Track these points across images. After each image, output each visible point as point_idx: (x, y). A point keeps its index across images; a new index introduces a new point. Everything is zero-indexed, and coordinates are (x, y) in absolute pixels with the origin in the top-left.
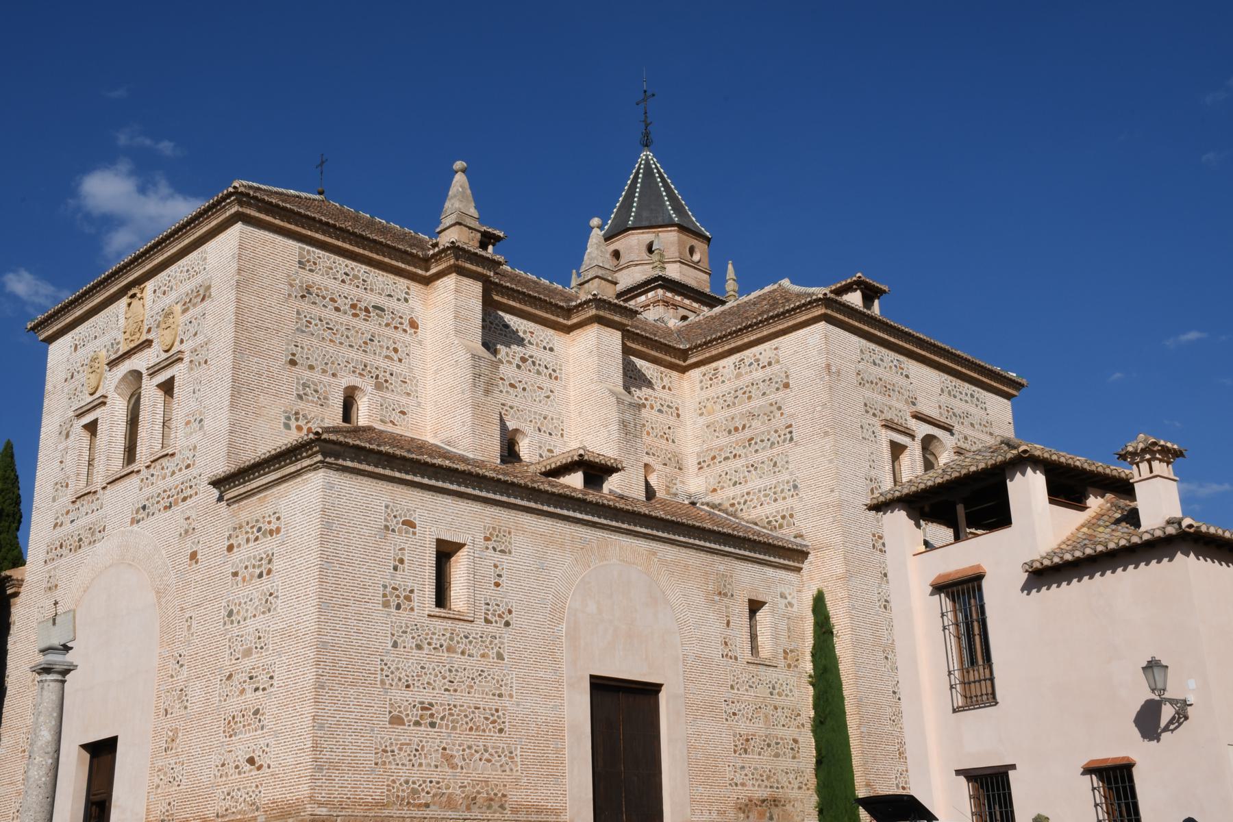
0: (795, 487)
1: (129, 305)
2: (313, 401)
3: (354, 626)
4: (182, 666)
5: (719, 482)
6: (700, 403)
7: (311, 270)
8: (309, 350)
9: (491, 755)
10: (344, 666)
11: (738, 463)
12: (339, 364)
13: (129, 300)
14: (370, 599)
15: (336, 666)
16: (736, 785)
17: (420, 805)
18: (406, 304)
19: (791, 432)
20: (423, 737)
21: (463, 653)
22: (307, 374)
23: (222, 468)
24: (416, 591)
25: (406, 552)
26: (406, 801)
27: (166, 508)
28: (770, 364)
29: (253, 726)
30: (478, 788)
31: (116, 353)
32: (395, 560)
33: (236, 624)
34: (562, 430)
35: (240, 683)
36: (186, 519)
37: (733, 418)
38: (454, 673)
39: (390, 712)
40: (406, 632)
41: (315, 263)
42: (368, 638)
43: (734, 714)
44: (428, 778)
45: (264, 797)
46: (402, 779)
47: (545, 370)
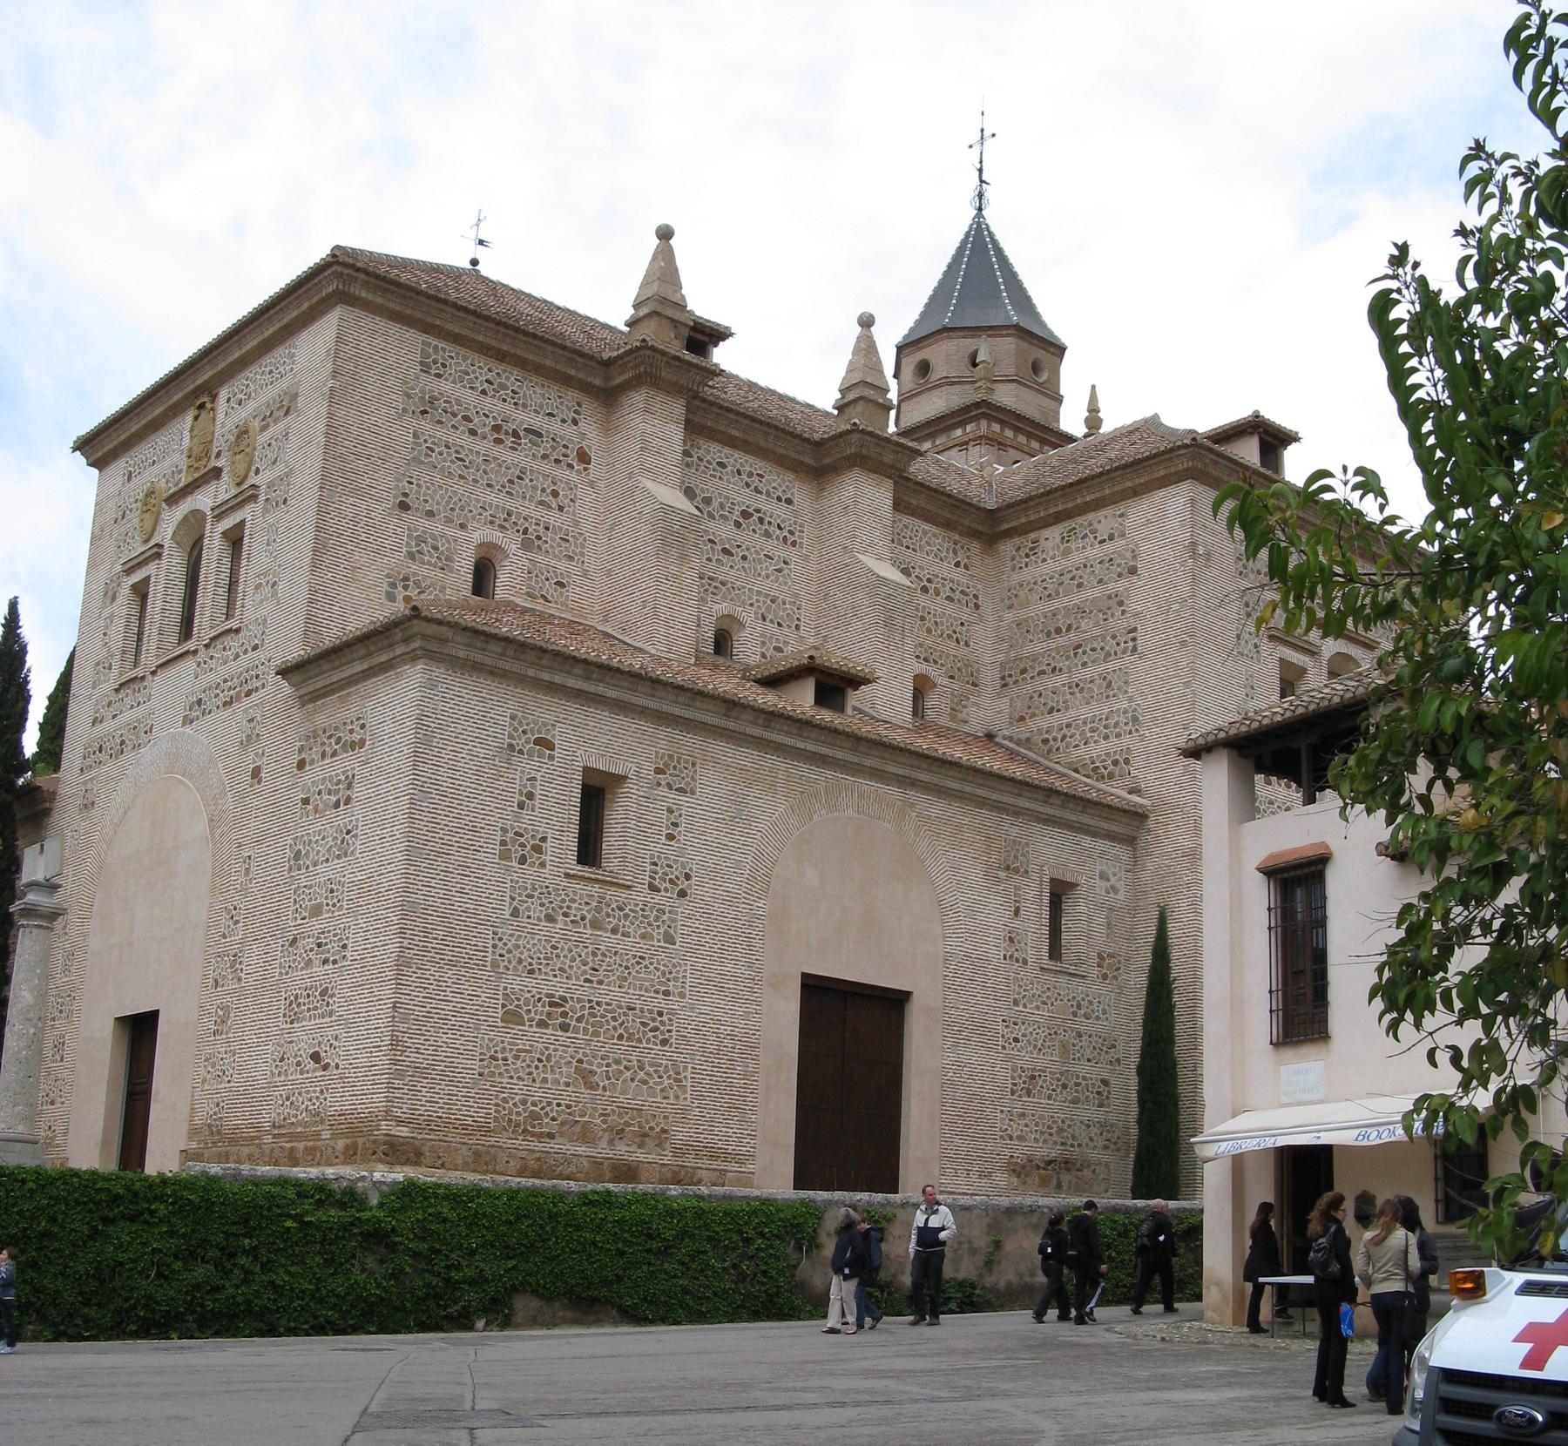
0: (1135, 719)
1: (196, 418)
2: (430, 563)
3: (457, 883)
4: (237, 922)
5: (1030, 707)
6: (1009, 590)
7: (438, 376)
8: (428, 488)
9: (648, 1074)
10: (440, 937)
11: (1059, 680)
12: (471, 511)
13: (196, 412)
14: (482, 847)
15: (427, 937)
16: (1011, 1138)
17: (540, 1136)
18: (575, 428)
19: (1134, 639)
20: (551, 1044)
21: (614, 931)
22: (425, 523)
23: (295, 651)
24: (549, 840)
25: (538, 783)
26: (522, 1127)
27: (225, 704)
28: (1111, 537)
29: (320, 1011)
30: (626, 1119)
31: (177, 485)
32: (521, 794)
33: (303, 871)
34: (798, 619)
35: (306, 952)
36: (249, 721)
37: (1054, 615)
38: (599, 957)
39: (504, 1006)
40: (531, 896)
41: (444, 366)
42: (476, 900)
43: (1016, 1040)
44: (554, 1099)
45: (331, 1106)
46: (517, 1098)
47: (778, 532)
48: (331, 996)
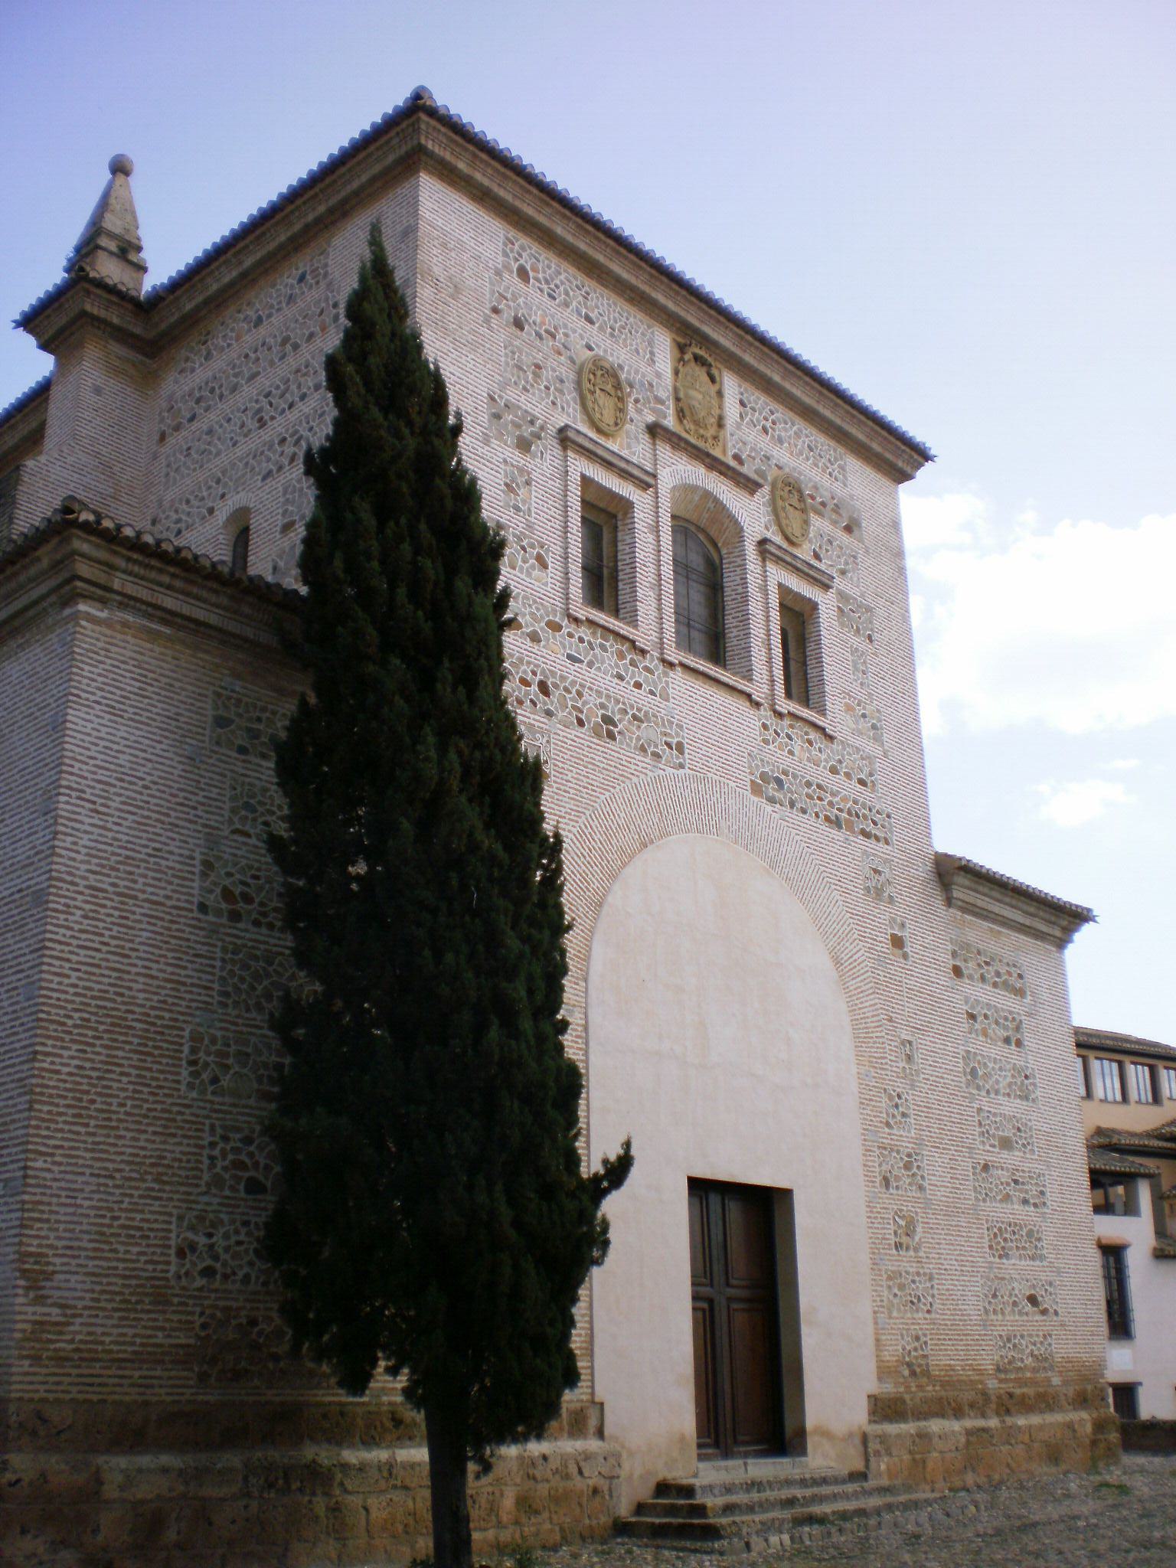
48: (1039, 1240)
